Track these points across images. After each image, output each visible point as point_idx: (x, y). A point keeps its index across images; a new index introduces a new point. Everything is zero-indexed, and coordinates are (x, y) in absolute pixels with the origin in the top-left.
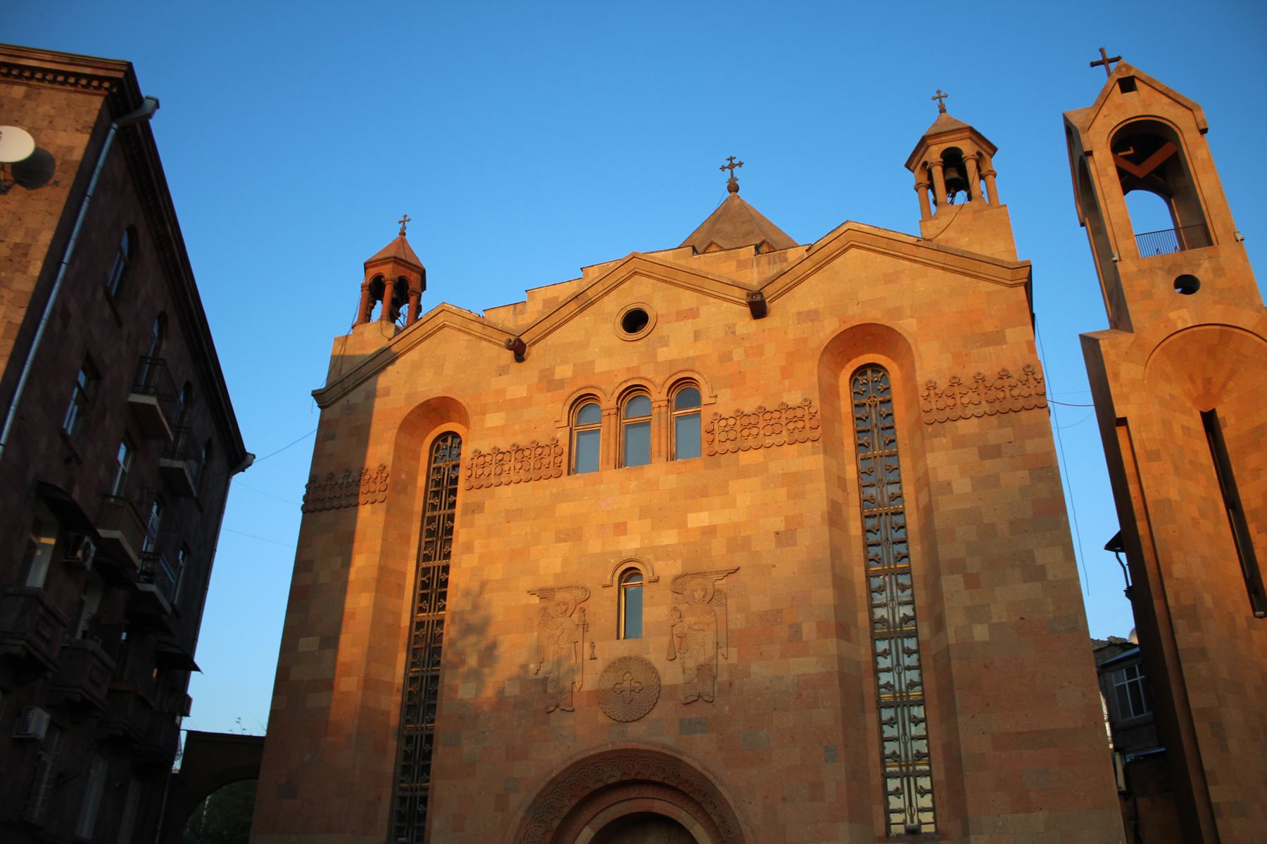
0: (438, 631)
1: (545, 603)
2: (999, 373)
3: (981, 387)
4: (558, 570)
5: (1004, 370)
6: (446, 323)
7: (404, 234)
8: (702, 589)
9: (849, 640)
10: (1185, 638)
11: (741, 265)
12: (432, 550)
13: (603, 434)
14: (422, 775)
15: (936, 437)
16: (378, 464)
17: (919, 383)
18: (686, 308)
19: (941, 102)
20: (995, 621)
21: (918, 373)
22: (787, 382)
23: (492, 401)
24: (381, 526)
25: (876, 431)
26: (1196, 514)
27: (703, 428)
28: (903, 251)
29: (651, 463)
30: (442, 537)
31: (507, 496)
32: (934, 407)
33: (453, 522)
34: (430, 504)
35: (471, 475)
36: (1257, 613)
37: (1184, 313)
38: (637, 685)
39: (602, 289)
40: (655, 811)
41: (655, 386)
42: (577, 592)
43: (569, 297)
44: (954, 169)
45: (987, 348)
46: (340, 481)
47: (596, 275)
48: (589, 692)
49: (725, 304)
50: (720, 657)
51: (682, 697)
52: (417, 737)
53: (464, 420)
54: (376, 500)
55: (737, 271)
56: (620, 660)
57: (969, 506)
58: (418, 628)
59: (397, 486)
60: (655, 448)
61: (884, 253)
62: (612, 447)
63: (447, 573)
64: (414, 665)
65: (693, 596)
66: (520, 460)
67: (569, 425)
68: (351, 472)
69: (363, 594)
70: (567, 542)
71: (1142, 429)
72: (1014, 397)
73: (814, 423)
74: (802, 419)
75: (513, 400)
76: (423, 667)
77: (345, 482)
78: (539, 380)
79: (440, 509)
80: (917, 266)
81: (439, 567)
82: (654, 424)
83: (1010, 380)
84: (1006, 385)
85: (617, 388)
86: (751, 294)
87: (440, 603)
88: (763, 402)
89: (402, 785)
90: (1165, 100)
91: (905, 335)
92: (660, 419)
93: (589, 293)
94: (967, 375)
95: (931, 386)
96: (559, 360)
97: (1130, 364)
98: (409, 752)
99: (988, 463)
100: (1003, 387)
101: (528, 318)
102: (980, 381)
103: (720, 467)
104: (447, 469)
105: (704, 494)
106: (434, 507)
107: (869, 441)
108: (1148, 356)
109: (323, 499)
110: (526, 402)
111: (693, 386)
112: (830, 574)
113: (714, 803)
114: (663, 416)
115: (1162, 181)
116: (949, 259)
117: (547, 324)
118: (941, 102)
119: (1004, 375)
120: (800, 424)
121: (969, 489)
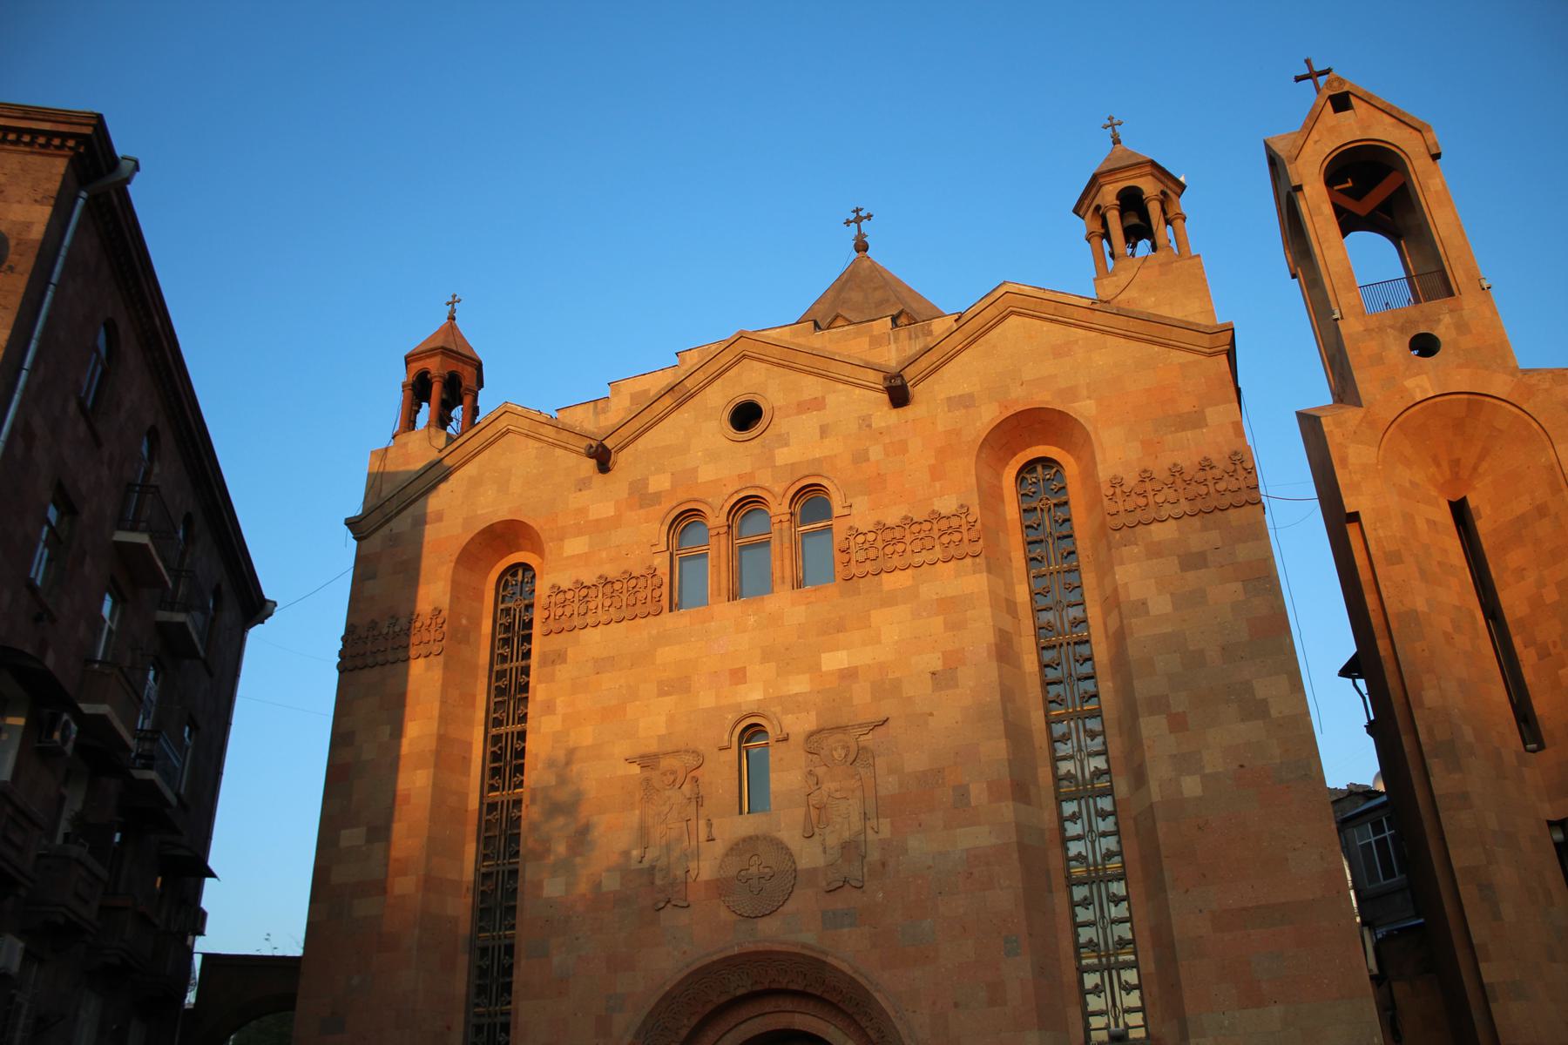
0: (515, 813)
1: (647, 773)
2: (1200, 463)
3: (1179, 481)
4: (663, 731)
5: (1206, 459)
6: (510, 427)
7: (454, 319)
8: (843, 747)
9: (1028, 803)
10: (1443, 781)
11: (876, 342)
12: (504, 712)
13: (712, 559)
14: (502, 996)
15: (1125, 546)
16: (432, 608)
17: (1101, 480)
18: (810, 397)
19: (1114, 130)
20: (1207, 771)
21: (1100, 467)
22: (938, 485)
23: (572, 522)
24: (438, 684)
25: (1050, 541)
26: (1449, 629)
27: (836, 547)
28: (1075, 317)
29: (772, 592)
30: (515, 695)
31: (594, 640)
32: (1122, 509)
33: (528, 675)
34: (498, 655)
35: (549, 617)
36: (1528, 746)
37: (1423, 380)
38: (767, 870)
39: (703, 378)
40: (796, 1028)
41: (774, 495)
42: (687, 757)
43: (662, 389)
44: (1133, 213)
45: (1184, 433)
46: (385, 631)
47: (695, 361)
48: (707, 883)
49: (857, 391)
50: (869, 831)
51: (824, 883)
52: (493, 948)
53: (538, 549)
54: (430, 653)
55: (870, 349)
56: (744, 840)
57: (1170, 630)
58: (489, 813)
59: (456, 635)
60: (777, 574)
61: (1052, 321)
62: (724, 575)
63: (524, 740)
64: (486, 857)
65: (833, 756)
66: (610, 595)
67: (668, 549)
68: (397, 619)
69: (419, 772)
70: (671, 695)
71: (1378, 525)
72: (1220, 492)
73: (974, 535)
74: (958, 530)
75: (597, 520)
76: (504, 859)
77: (391, 632)
78: (629, 494)
79: (512, 661)
80: (1093, 334)
81: (513, 733)
82: (775, 544)
83: (1214, 471)
84: (1210, 478)
85: (726, 501)
86: (889, 377)
87: (516, 779)
88: (910, 511)
89: (476, 1010)
90: (1388, 120)
91: (1082, 421)
92: (781, 537)
93: (688, 384)
94: (1160, 468)
95: (1116, 483)
96: (653, 468)
97: (1360, 446)
98: (485, 967)
99: (1191, 575)
100: (1205, 480)
101: (612, 418)
102: (1177, 474)
103: (860, 594)
104: (518, 610)
105: (841, 628)
106: (504, 659)
107: (1044, 554)
108: (1381, 435)
109: (364, 654)
110: (615, 522)
111: (822, 495)
112: (1002, 721)
113: (870, 1014)
114: (786, 534)
115: (1389, 218)
116: (1134, 325)
117: (636, 424)
118: (1114, 130)
119: (1206, 465)
120: (956, 537)
121: (1169, 609)
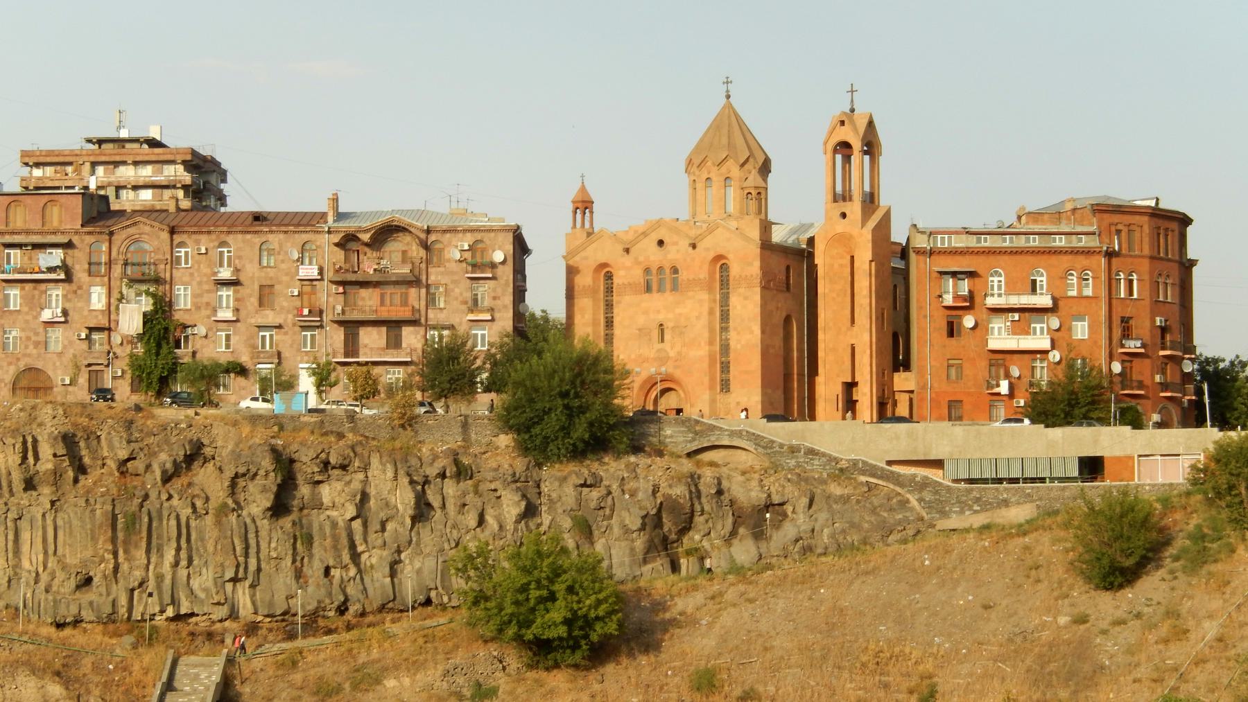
101: (630, 237)
